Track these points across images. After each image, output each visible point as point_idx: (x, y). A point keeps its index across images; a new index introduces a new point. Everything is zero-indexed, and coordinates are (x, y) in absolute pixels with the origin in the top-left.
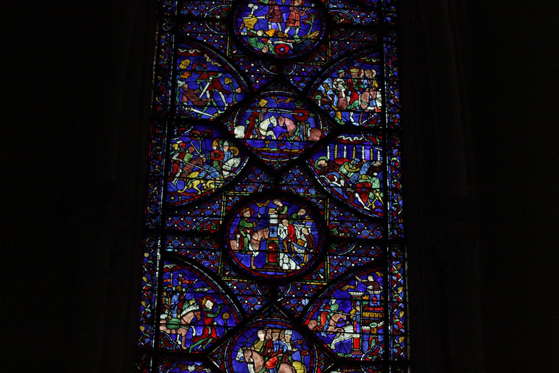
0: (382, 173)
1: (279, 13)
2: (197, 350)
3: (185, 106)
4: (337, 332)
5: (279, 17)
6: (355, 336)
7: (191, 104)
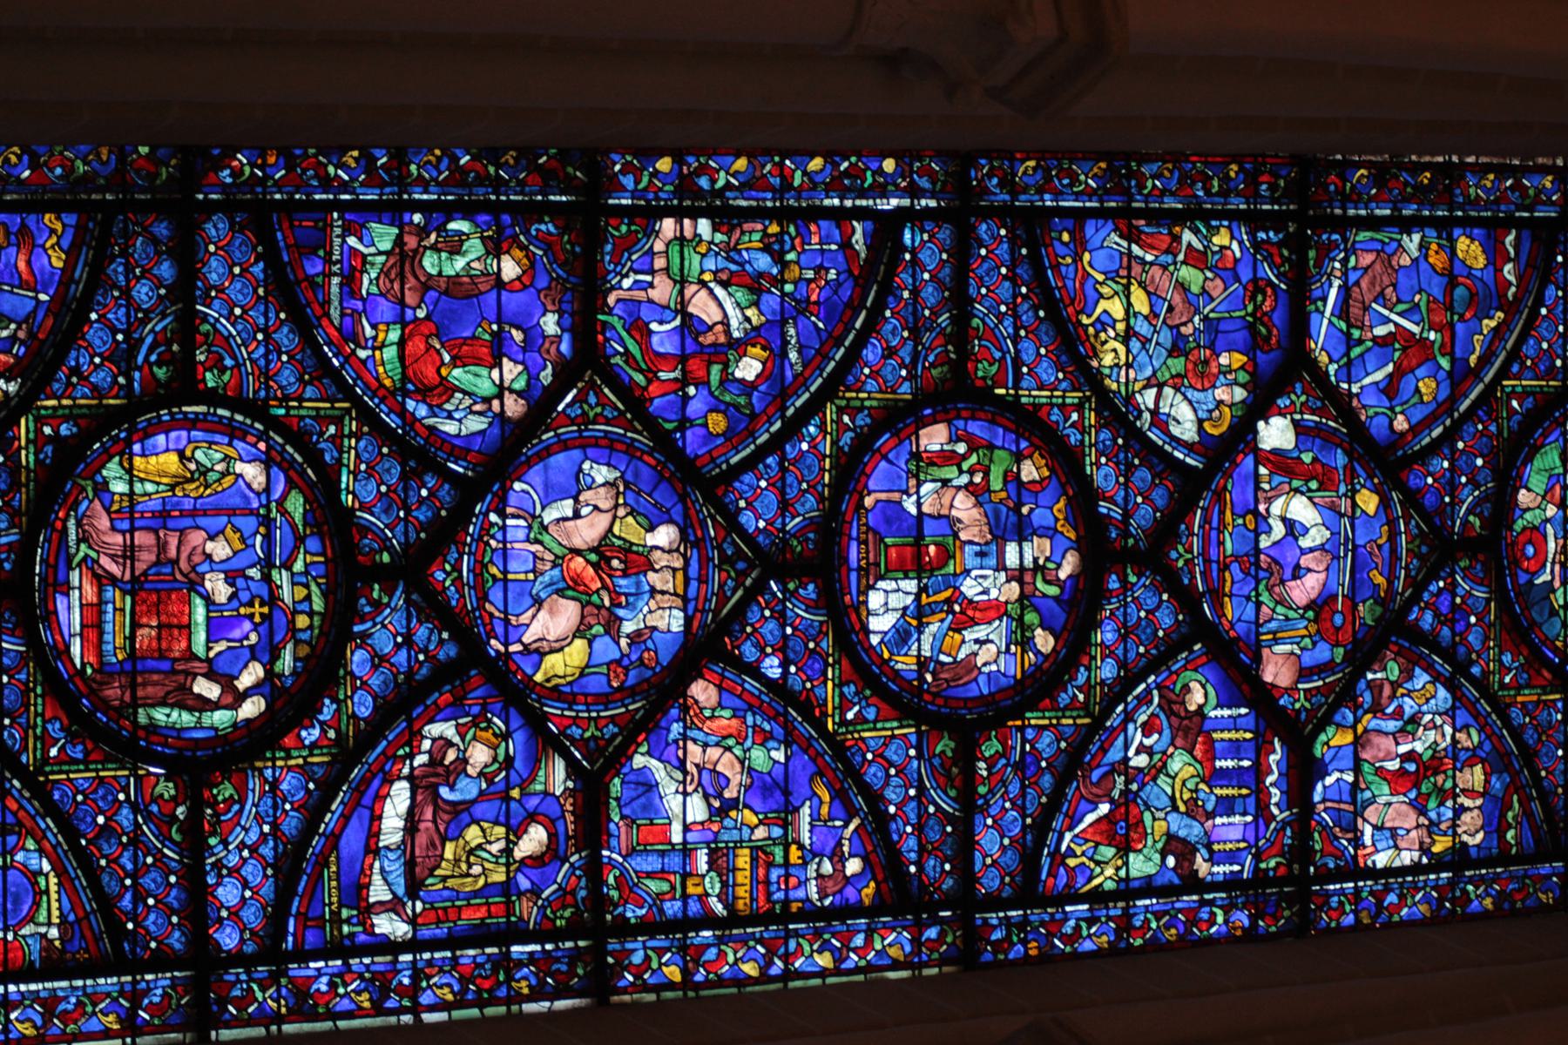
0: (1176, 881)
2: (607, 340)
3: (1345, 261)
7: (1353, 277)
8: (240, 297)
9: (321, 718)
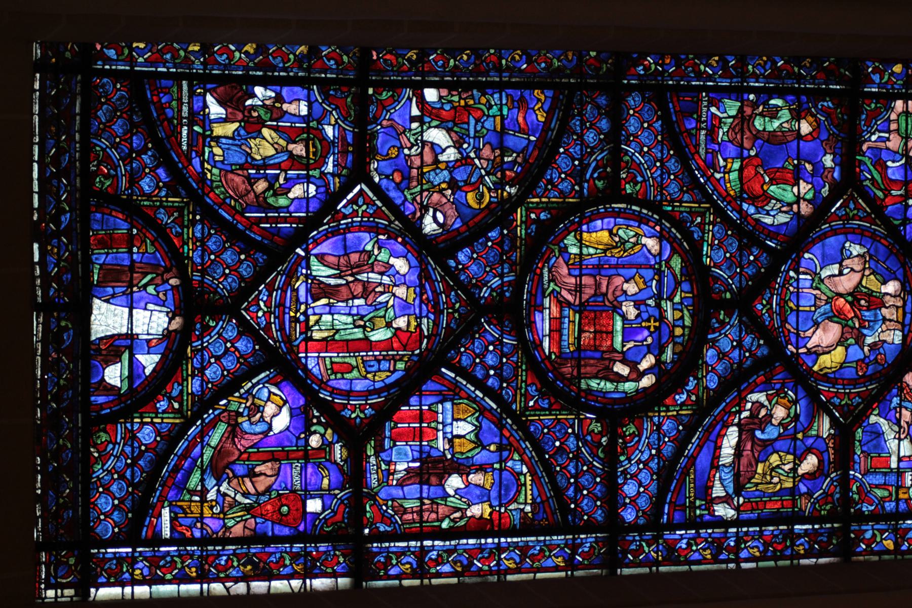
2: (862, 171)
4: (900, 427)
6: (894, 459)
8: (647, 141)
9: (688, 388)
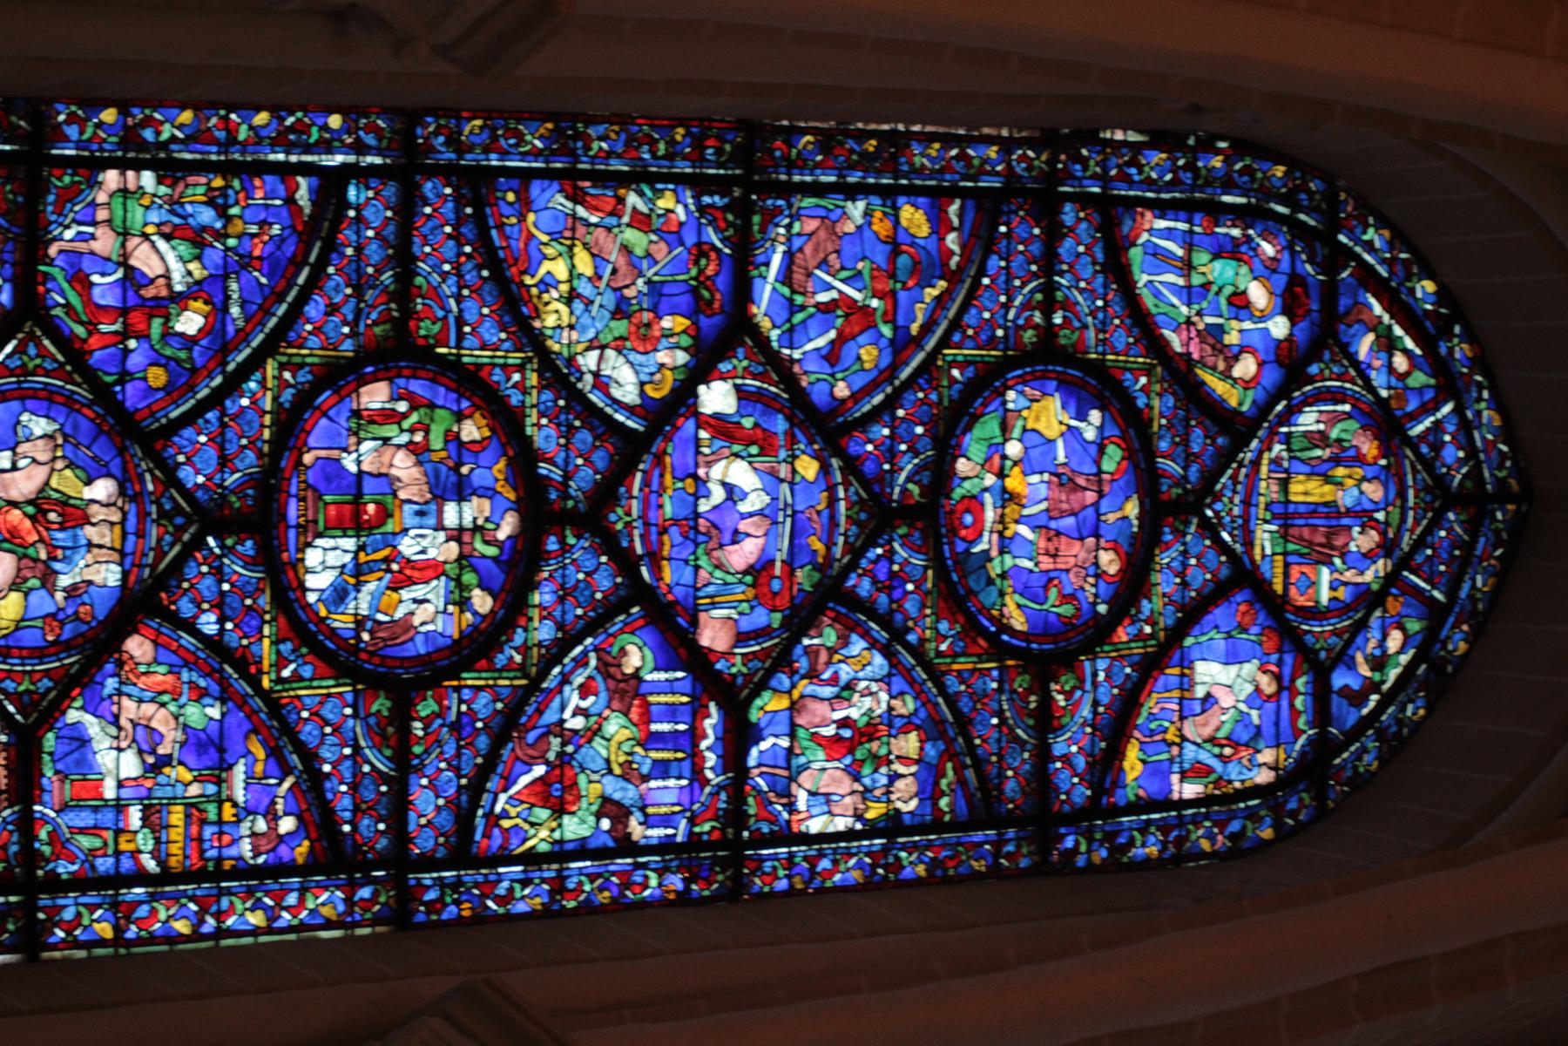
0: (611, 843)
1: (1076, 507)
2: (48, 291)
3: (789, 227)
4: (120, 728)
5: (1065, 506)
7: (797, 243)
